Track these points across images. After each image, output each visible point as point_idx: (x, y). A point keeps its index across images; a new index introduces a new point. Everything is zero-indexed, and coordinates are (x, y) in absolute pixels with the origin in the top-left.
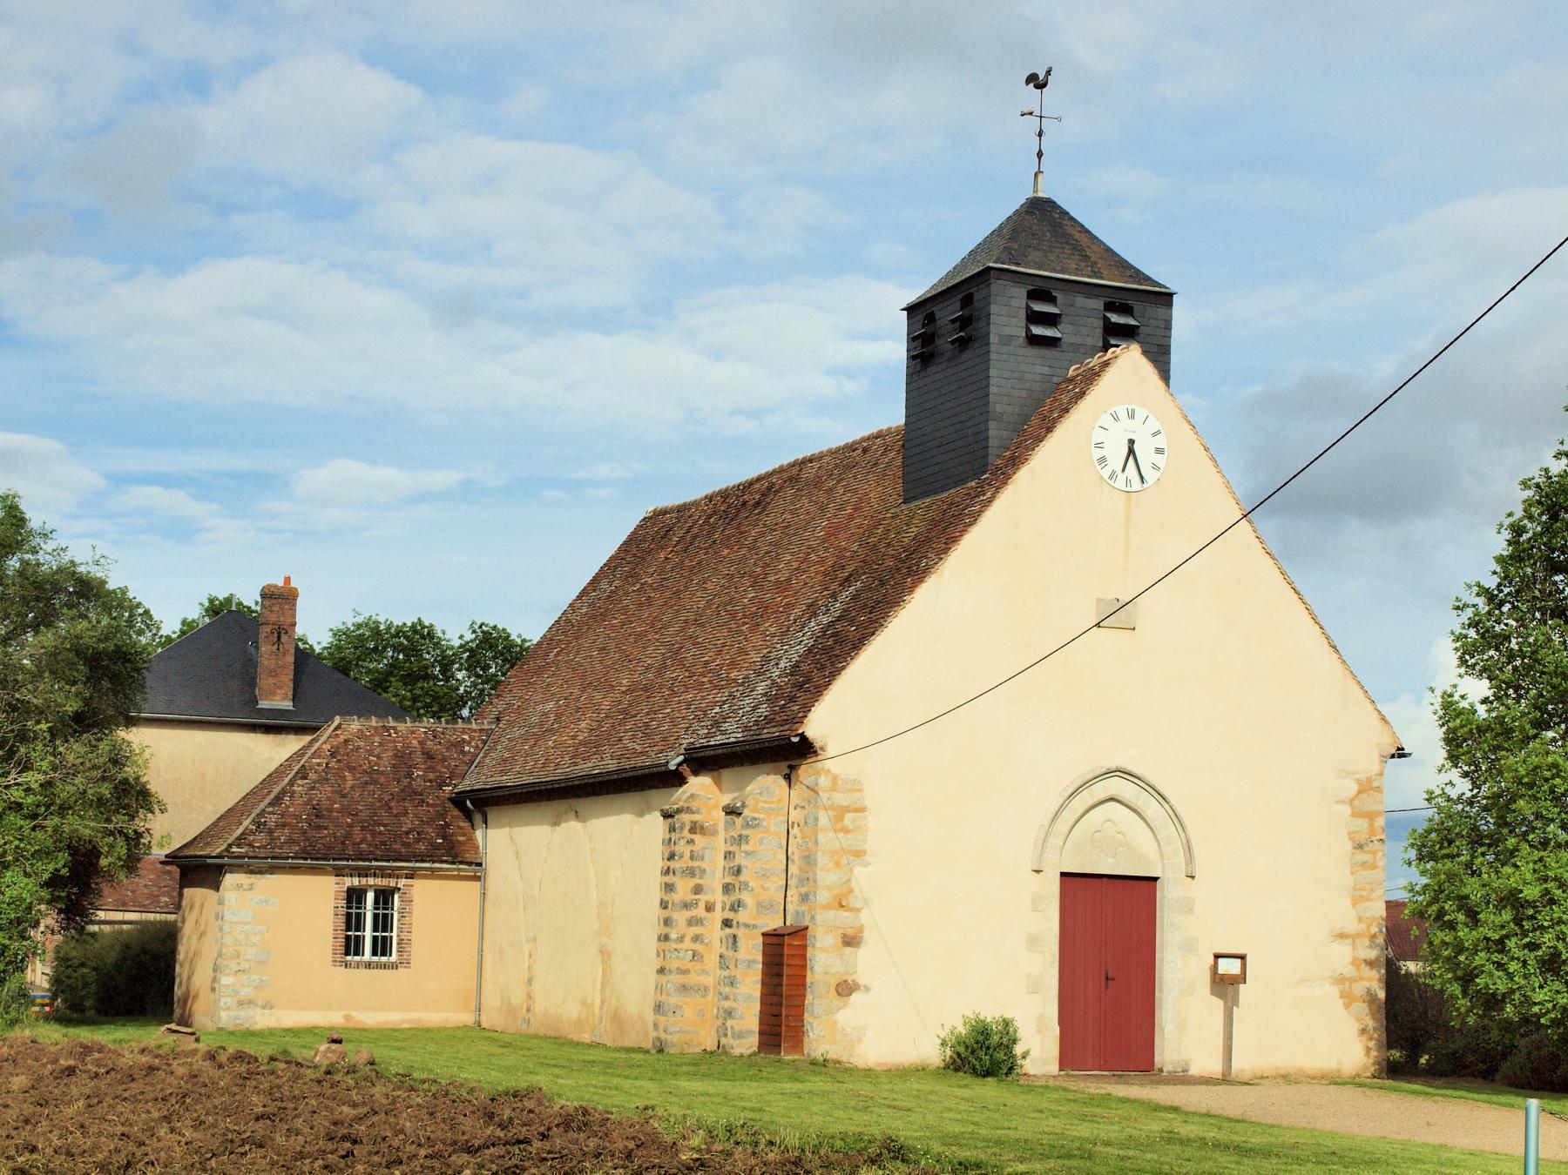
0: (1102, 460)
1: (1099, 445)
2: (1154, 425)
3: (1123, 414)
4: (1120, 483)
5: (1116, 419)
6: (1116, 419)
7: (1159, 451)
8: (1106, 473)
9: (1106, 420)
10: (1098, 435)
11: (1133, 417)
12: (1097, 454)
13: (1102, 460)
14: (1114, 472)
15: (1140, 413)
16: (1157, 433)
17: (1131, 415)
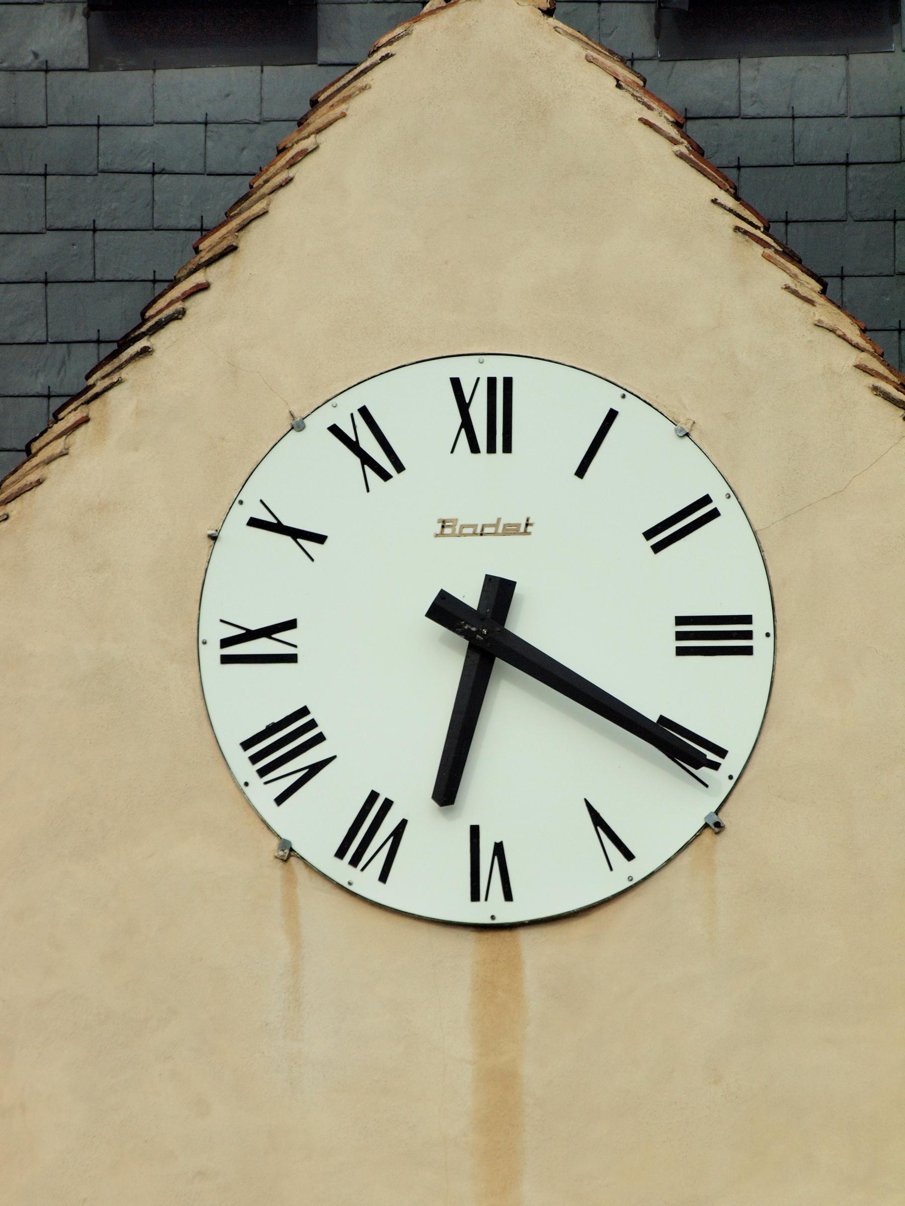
0: (286, 745)
1: (257, 644)
2: (655, 469)
4: (430, 873)
5: (377, 457)
6: (377, 457)
8: (317, 820)
9: (309, 476)
10: (250, 581)
11: (500, 436)
12: (249, 700)
13: (286, 745)
14: (375, 808)
15: (553, 407)
16: (665, 534)
17: (488, 419)
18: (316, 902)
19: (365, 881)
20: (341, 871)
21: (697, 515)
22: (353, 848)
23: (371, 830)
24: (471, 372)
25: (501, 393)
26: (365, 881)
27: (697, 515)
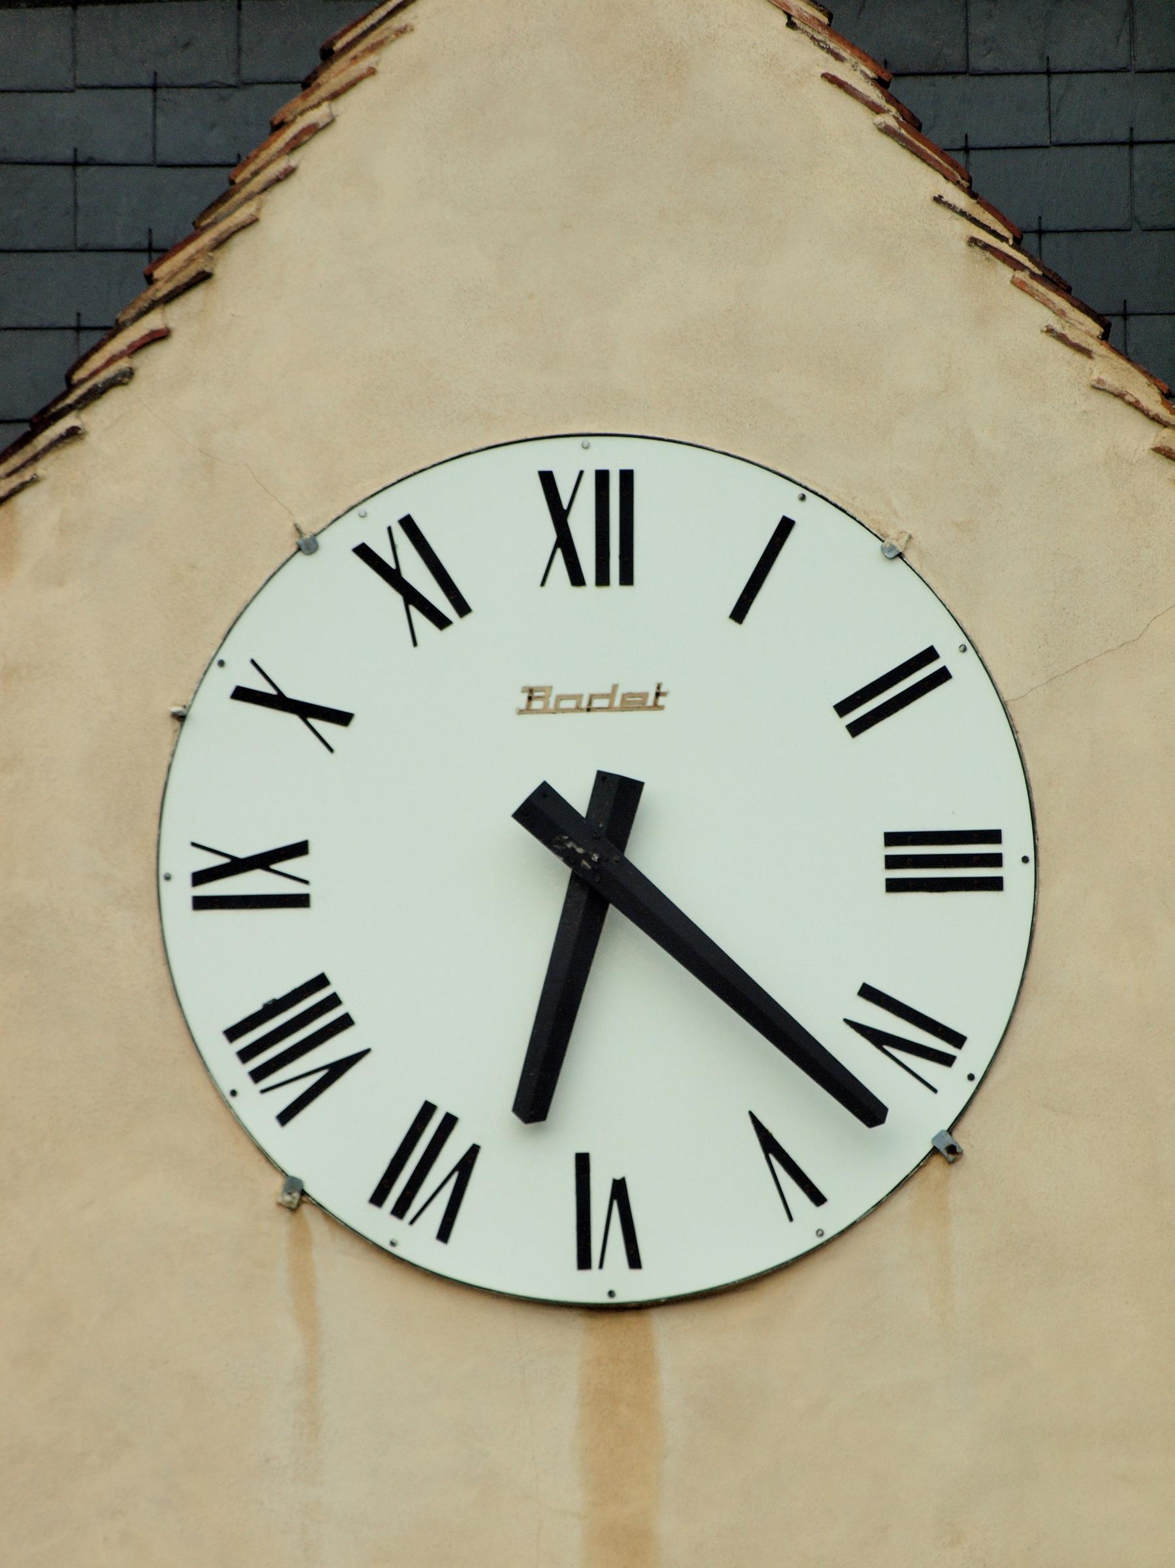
0: (296, 1031)
1: (249, 880)
2: (852, 607)
3: (490, 525)
4: (515, 1229)
5: (428, 592)
6: (428, 592)
7: (938, 862)
8: (341, 1146)
11: (617, 561)
12: (236, 965)
13: (296, 1031)
14: (430, 1127)
15: (696, 517)
17: (599, 537)
18: (338, 1268)
19: (416, 1240)
20: (380, 1225)
21: (915, 679)
22: (396, 1189)
23: (424, 1162)
24: (571, 463)
25: (617, 493)
26: (416, 1240)
27: (915, 679)
